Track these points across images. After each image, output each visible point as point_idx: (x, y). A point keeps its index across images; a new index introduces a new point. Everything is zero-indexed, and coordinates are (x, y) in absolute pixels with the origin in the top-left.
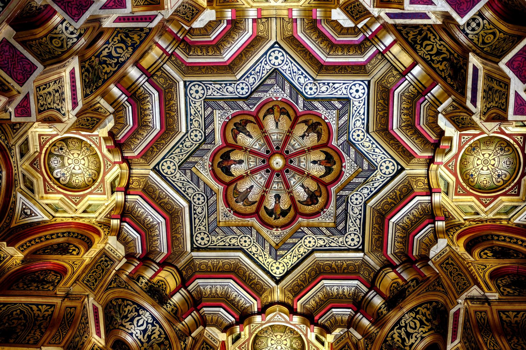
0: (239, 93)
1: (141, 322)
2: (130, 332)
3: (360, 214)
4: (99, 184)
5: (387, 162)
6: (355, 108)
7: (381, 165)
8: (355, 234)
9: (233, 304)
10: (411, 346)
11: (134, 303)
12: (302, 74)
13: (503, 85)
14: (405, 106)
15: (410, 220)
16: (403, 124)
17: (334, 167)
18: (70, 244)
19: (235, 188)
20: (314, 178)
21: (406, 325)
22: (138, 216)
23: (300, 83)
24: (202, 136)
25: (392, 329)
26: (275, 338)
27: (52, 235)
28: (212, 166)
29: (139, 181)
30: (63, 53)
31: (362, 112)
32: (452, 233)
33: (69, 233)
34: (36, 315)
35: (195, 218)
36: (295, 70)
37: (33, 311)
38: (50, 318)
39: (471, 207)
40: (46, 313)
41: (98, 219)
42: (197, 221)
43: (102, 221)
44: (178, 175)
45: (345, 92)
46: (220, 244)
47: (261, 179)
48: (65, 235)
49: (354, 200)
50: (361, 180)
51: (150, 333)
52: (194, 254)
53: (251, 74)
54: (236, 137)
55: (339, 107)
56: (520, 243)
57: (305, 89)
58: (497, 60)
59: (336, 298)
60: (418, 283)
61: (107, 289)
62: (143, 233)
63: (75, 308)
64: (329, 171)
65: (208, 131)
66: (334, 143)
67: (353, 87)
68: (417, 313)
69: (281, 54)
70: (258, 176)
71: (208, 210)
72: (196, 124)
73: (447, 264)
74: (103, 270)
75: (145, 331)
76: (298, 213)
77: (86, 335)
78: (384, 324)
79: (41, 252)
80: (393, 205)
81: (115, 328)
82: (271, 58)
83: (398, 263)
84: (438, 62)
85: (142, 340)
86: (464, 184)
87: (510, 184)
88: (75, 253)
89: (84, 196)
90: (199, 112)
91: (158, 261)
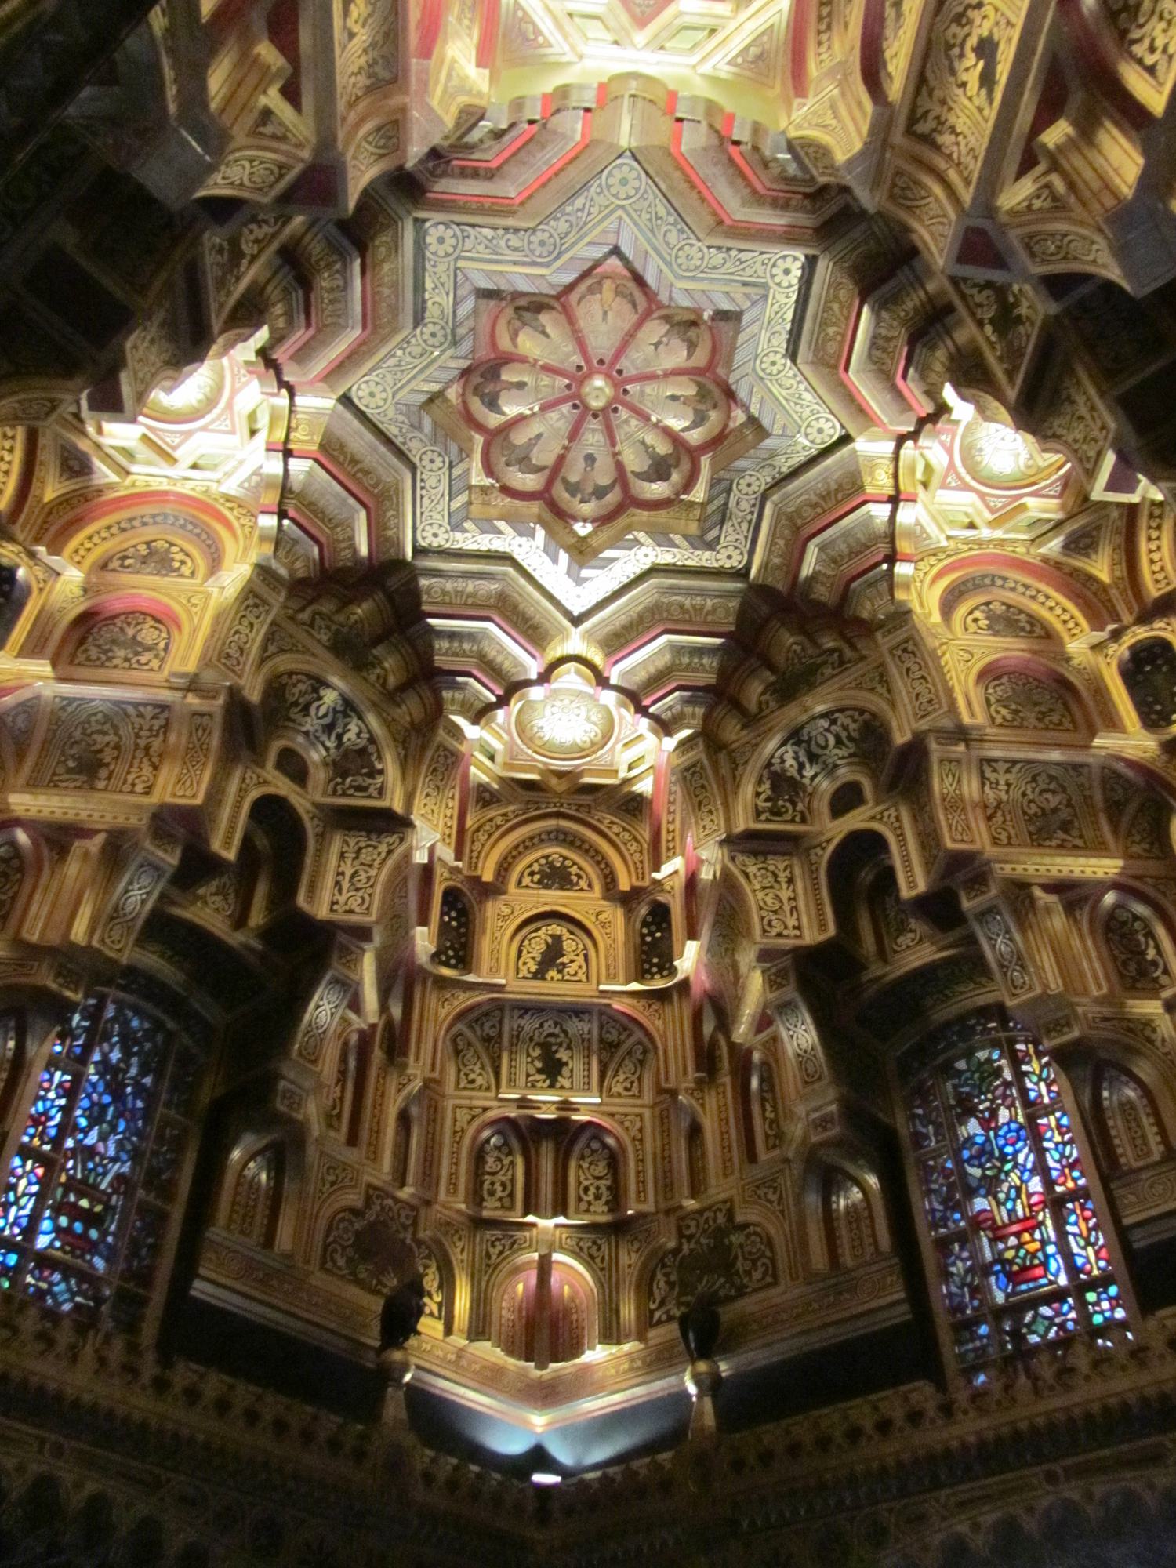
2: (304, 729)
3: (752, 513)
7: (809, 426)
9: (493, 669)
11: (309, 676)
13: (1099, 423)
15: (849, 546)
18: (172, 545)
19: (506, 438)
20: (667, 432)
23: (667, 243)
24: (445, 336)
25: (784, 744)
27: (131, 520)
28: (463, 395)
31: (789, 316)
35: (422, 497)
38: (165, 733)
39: (966, 514)
41: (224, 489)
42: (426, 501)
43: (233, 493)
47: (560, 419)
48: (159, 519)
49: (743, 487)
51: (339, 730)
56: (1041, 599)
60: (842, 662)
61: (262, 661)
62: (323, 539)
63: (210, 715)
64: (699, 420)
66: (721, 371)
68: (834, 722)
69: (634, 174)
71: (450, 486)
72: (432, 311)
73: (905, 650)
74: (252, 625)
75: (329, 728)
76: (630, 501)
79: (115, 564)
80: (819, 510)
81: (277, 727)
84: (975, 285)
86: (962, 471)
87: (1050, 476)
88: (186, 570)
89: (189, 434)
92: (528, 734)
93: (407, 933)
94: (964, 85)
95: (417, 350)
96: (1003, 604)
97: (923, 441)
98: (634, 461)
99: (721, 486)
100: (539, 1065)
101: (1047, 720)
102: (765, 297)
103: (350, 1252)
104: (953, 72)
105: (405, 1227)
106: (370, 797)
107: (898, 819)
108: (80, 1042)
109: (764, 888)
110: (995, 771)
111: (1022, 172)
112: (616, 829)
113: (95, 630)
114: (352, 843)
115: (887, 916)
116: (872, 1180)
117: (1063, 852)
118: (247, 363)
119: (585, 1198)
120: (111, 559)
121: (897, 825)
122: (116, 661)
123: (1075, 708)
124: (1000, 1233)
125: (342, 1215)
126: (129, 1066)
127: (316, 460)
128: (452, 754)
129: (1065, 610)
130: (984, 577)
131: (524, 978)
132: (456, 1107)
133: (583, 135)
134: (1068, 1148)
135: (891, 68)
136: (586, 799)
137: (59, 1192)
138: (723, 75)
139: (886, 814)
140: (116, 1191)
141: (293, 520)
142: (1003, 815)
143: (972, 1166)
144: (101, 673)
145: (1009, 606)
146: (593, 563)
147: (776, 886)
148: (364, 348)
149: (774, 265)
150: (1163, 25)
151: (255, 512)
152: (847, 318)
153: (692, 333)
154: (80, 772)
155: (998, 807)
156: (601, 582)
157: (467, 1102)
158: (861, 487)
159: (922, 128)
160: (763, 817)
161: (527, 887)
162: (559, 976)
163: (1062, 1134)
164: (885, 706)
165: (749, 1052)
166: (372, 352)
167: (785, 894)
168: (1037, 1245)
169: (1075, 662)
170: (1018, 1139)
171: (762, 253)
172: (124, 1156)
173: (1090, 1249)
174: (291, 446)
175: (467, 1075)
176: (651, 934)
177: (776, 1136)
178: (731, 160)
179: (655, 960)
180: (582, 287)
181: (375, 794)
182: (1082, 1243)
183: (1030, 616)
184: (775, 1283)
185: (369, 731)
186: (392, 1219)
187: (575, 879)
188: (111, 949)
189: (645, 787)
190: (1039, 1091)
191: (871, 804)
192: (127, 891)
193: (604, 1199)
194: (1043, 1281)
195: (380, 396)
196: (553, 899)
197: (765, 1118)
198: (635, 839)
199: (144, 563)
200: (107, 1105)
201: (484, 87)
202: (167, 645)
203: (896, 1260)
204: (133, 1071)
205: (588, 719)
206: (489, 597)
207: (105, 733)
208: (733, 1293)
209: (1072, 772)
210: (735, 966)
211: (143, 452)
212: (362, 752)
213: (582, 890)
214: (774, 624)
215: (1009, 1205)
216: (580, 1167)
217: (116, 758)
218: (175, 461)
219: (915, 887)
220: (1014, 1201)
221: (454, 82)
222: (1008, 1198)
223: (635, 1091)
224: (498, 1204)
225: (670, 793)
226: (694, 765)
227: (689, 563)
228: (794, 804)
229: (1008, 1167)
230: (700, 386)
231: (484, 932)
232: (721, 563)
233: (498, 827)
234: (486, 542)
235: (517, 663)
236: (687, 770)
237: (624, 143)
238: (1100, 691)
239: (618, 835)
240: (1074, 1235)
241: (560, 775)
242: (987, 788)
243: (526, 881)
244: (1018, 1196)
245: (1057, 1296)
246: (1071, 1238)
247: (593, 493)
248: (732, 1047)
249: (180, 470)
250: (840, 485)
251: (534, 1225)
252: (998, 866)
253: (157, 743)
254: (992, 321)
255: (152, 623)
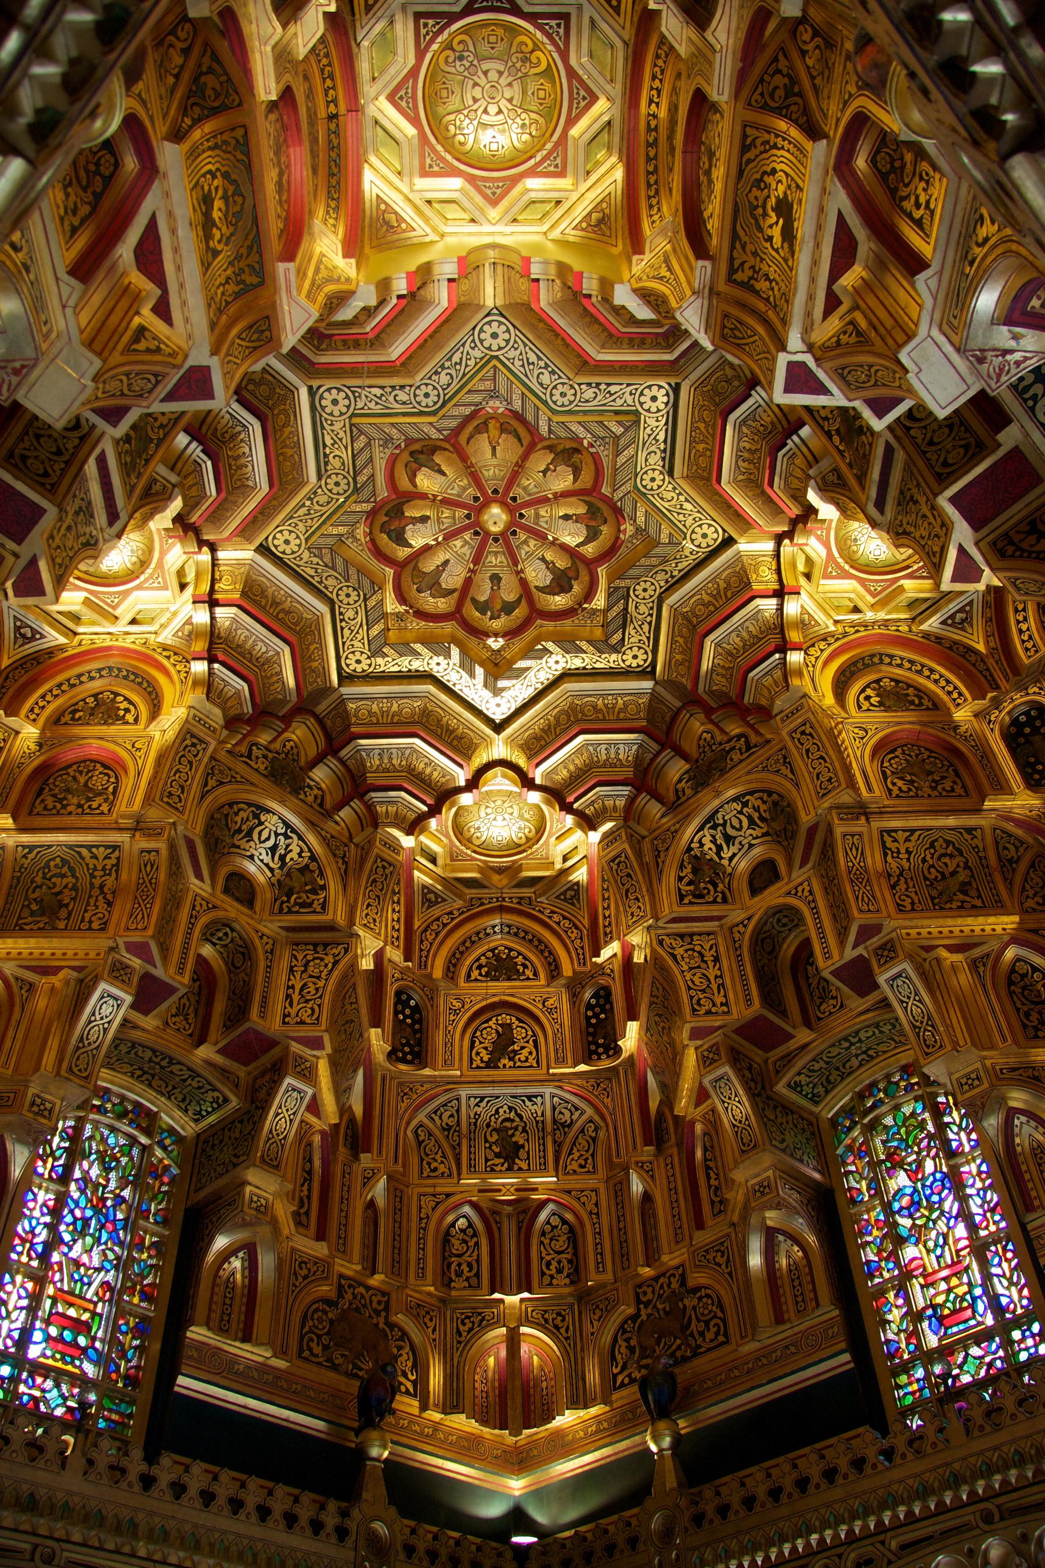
0: (419, 403)
1: (265, 835)
3: (651, 615)
4: (155, 569)
5: (705, 527)
6: (648, 431)
7: (693, 532)
8: (640, 648)
9: (423, 781)
10: (731, 859)
11: (249, 805)
12: (547, 366)
14: (747, 446)
15: (742, 639)
16: (741, 477)
17: (604, 529)
18: (117, 694)
19: (416, 568)
20: (564, 548)
21: (725, 822)
22: (238, 646)
23: (541, 384)
24: (348, 484)
26: (492, 805)
28: (371, 533)
29: (232, 574)
30: (82, 439)
31: (661, 437)
32: (813, 659)
33: (110, 669)
34: (91, 866)
35: (342, 628)
36: (533, 358)
37: (83, 859)
38: (117, 871)
39: (850, 599)
40: (107, 861)
41: (160, 639)
42: (346, 632)
43: (169, 642)
44: (306, 555)
45: (630, 402)
46: (392, 669)
47: (462, 547)
48: (104, 673)
50: (654, 561)
52: (344, 690)
53: (443, 367)
54: (415, 476)
55: (619, 433)
56: (927, 673)
57: (551, 395)
58: (936, 487)
59: (604, 766)
60: (748, 747)
62: (252, 677)
63: (157, 851)
64: (592, 535)
65: (361, 479)
66: (605, 490)
67: (646, 392)
68: (745, 804)
70: (458, 543)
72: (336, 463)
73: (803, 733)
74: (191, 763)
75: (273, 849)
76: (537, 613)
77: (180, 886)
78: (688, 816)
79: (67, 717)
80: (712, 608)
82: (482, 336)
83: (714, 705)
85: (272, 865)
86: (840, 560)
88: (130, 718)
89: (126, 594)
90: (341, 440)
91: (281, 714)
92: (467, 835)
93: (361, 1035)
94: (770, 239)
95: (323, 499)
96: (892, 680)
97: (799, 539)
98: (537, 575)
99: (619, 595)
100: (497, 1150)
101: (939, 788)
102: (637, 422)
103: (325, 1340)
104: (760, 229)
105: (378, 1313)
106: (314, 912)
107: (811, 892)
108: (61, 1162)
109: (691, 969)
110: (895, 840)
111: (827, 313)
112: (556, 918)
113: (51, 780)
114: (300, 957)
115: (810, 985)
116: (811, 1239)
117: (963, 913)
118: (166, 530)
119: (548, 1272)
120: (63, 714)
121: (811, 898)
122: (70, 808)
123: (964, 774)
124: (930, 1279)
125: (316, 1306)
126: (108, 1180)
127: (239, 607)
128: (390, 864)
129: (948, 682)
130: (872, 656)
131: (478, 1067)
132: (421, 1195)
133: (450, 301)
134: (989, 1194)
135: (709, 227)
136: (527, 892)
137: (48, 1303)
138: (571, 239)
139: (800, 889)
140: (100, 1299)
141: (223, 664)
142: (906, 883)
143: (902, 1216)
144: (57, 821)
145: (897, 682)
146: (508, 674)
147: (703, 965)
148: (275, 503)
149: (642, 394)
150: (923, 184)
151: (189, 657)
152: (713, 436)
153: (576, 458)
154: (43, 914)
155: (901, 874)
156: (517, 691)
157: (431, 1190)
158: (748, 584)
159: (739, 276)
160: (686, 901)
161: (476, 980)
162: (511, 1063)
163: (983, 1180)
164: (789, 785)
165: (692, 1123)
166: (282, 505)
167: (712, 973)
168: (965, 1288)
169: (963, 729)
170: (943, 1187)
171: (628, 385)
172: (108, 1266)
173: (1013, 1289)
174: (217, 596)
175: (429, 1164)
176: (596, 1016)
177: (721, 1202)
178: (585, 309)
179: (601, 1041)
180: (470, 428)
181: (319, 909)
182: (1005, 1283)
183: (918, 690)
184: (727, 1342)
185: (310, 850)
186: (365, 1306)
187: (521, 969)
188: (78, 1076)
189: (580, 875)
190: (960, 1140)
191: (786, 880)
192: (90, 1022)
193: (565, 1273)
194: (972, 1322)
195: (294, 542)
196: (500, 989)
197: (710, 1186)
198: (577, 928)
199: (91, 715)
200: (91, 1218)
201: (352, 273)
202: (115, 789)
203: (836, 1312)
204: (112, 1185)
205: (521, 817)
206: (413, 714)
207: (64, 876)
208: (688, 1354)
209: (966, 836)
210: (672, 1043)
211: (87, 614)
212: (304, 870)
213: (528, 979)
214: (684, 715)
215: (938, 1252)
216: (542, 1242)
217: (74, 899)
218: (116, 618)
219: (830, 957)
220: (942, 1247)
221: (323, 274)
222: (936, 1246)
223: (589, 1167)
224: (466, 1284)
225: (604, 880)
226: (619, 856)
227: (598, 665)
228: (715, 885)
229: (935, 1216)
230: (590, 505)
231: (437, 1027)
232: (628, 663)
233: (445, 925)
234: (406, 663)
235: (444, 773)
236: (613, 861)
237: (490, 303)
238: (986, 755)
239: (558, 923)
240: (998, 1276)
241: (500, 870)
242: (889, 858)
243: (475, 974)
244: (946, 1242)
245: (983, 1337)
246: (995, 1279)
247: (501, 610)
248: (676, 1118)
249: (122, 626)
250: (728, 584)
251: (502, 1301)
252: (904, 931)
253: (110, 882)
254: (838, 431)
255: (101, 769)
